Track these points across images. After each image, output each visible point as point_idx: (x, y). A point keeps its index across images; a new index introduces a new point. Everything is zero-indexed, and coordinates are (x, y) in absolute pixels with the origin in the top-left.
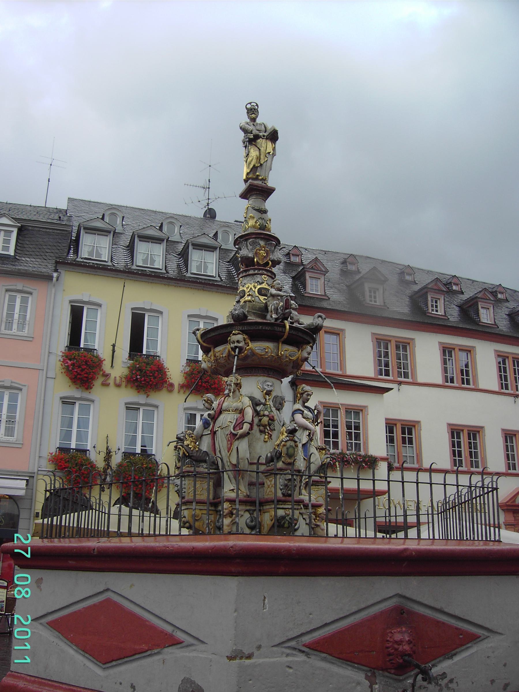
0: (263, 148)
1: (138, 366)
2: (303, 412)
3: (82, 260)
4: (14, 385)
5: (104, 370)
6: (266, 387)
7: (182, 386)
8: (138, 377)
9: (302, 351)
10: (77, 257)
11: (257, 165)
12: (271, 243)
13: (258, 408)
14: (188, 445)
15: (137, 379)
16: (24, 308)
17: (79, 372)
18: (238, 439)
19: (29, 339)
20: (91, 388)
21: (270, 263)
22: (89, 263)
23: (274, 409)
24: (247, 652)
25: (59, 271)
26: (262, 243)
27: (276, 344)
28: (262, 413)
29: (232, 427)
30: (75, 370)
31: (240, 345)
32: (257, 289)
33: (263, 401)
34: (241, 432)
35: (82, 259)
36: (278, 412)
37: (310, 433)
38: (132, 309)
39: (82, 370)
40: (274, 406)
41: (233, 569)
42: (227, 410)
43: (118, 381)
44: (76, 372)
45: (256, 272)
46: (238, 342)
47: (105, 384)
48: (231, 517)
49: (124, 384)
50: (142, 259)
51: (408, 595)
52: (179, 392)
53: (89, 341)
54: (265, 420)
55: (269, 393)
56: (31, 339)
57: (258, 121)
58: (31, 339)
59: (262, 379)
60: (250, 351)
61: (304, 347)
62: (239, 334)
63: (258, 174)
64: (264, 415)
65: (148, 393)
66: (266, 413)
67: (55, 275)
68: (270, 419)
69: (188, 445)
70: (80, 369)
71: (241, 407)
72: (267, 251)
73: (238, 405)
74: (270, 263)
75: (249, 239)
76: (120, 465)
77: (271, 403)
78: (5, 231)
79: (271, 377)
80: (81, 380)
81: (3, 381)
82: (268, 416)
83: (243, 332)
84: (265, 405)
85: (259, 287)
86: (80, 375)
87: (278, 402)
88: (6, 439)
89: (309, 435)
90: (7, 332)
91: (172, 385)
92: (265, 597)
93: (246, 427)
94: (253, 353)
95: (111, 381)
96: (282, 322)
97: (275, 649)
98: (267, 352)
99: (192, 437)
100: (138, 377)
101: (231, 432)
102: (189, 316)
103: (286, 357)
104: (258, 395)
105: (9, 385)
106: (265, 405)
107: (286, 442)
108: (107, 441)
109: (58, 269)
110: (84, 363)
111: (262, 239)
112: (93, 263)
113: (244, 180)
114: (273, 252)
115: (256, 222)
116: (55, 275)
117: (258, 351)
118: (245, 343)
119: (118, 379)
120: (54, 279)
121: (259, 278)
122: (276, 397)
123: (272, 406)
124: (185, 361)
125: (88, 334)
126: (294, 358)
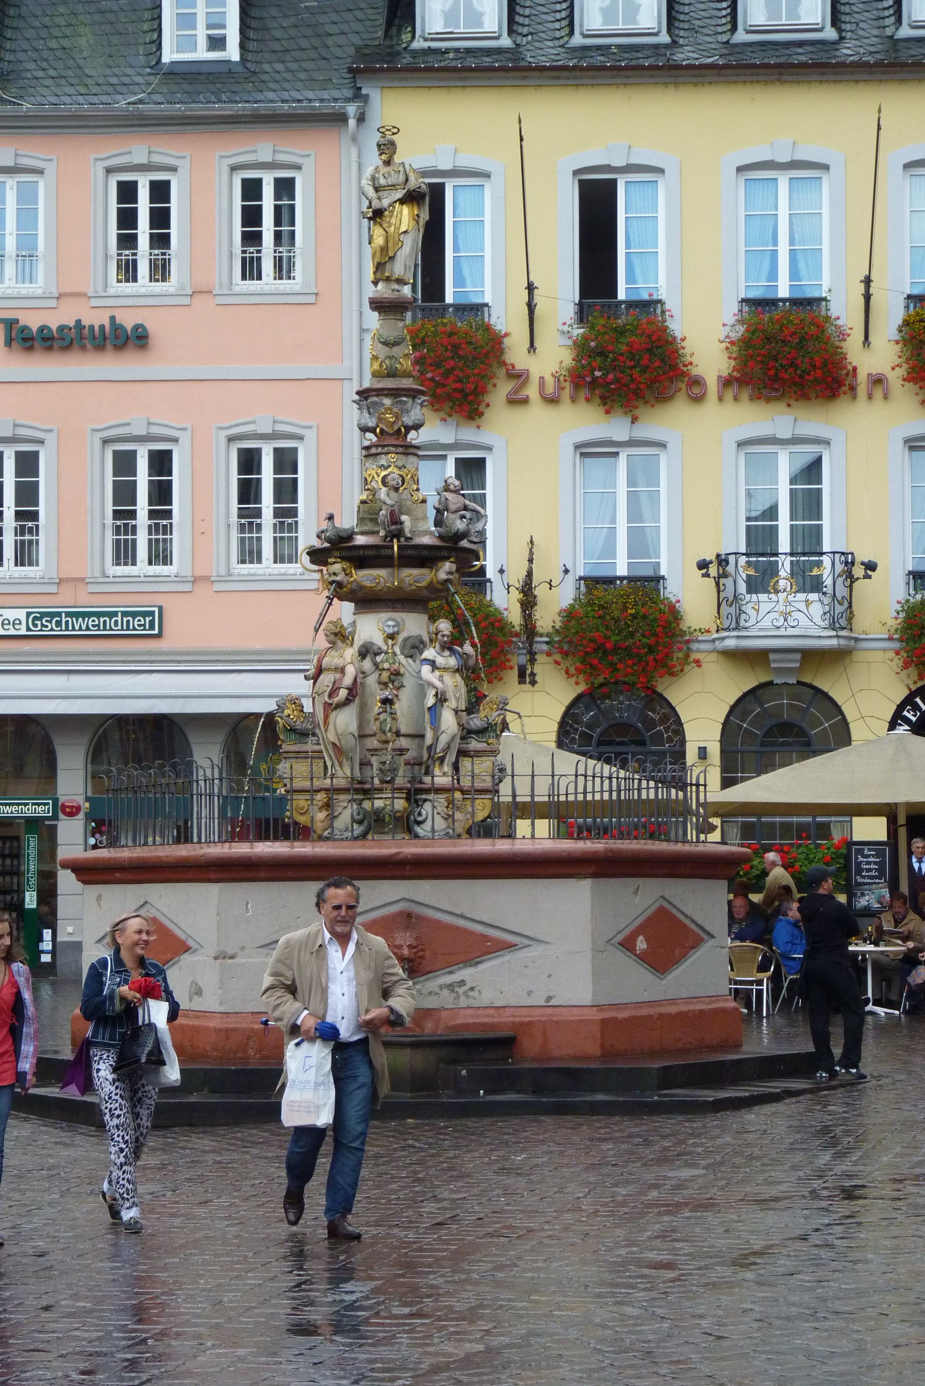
0: (393, 228)
1: (593, 344)
2: (434, 662)
3: (426, 45)
4: (280, 428)
5: (508, 361)
6: (387, 629)
7: (726, 382)
8: (598, 374)
9: (437, 571)
10: (413, 37)
11: (383, 261)
12: (401, 401)
13: (379, 659)
14: (289, 715)
15: (595, 379)
17: (437, 379)
18: (336, 708)
20: (481, 414)
21: (403, 430)
22: (447, 51)
23: (401, 658)
24: (230, 952)
25: (364, 91)
26: (387, 402)
27: (390, 570)
28: (381, 667)
29: (327, 694)
30: (429, 375)
31: (338, 578)
32: (380, 478)
33: (385, 648)
34: (336, 700)
35: (426, 40)
36: (410, 660)
37: (437, 693)
38: (575, 173)
39: (446, 375)
40: (402, 653)
41: (212, 876)
42: (328, 670)
43: (550, 388)
44: (432, 379)
45: (380, 450)
46: (335, 574)
47: (518, 401)
48: (327, 810)
49: (566, 394)
50: (601, 9)
51: (417, 899)
52: (721, 399)
53: (468, 282)
54: (385, 675)
55: (391, 636)
57: (397, 159)
59: (384, 616)
60: (355, 584)
61: (440, 564)
62: (335, 563)
63: (387, 274)
64: (384, 669)
65: (636, 412)
66: (386, 665)
67: (352, 109)
68: (392, 674)
69: (289, 715)
70: (442, 370)
71: (341, 665)
72: (396, 413)
73: (338, 662)
74: (403, 430)
75: (369, 396)
76: (569, 615)
77: (397, 649)
79: (398, 611)
80: (449, 397)
81: (254, 422)
82: (388, 669)
83: (343, 558)
84: (386, 653)
85: (384, 473)
86: (444, 386)
87: (408, 646)
88: (276, 572)
89: (436, 695)
91: (697, 382)
92: (248, 902)
93: (343, 693)
94: (362, 587)
95: (532, 391)
96: (392, 541)
97: (259, 950)
98: (378, 583)
99: (295, 703)
100: (598, 374)
101: (326, 703)
102: (740, 169)
103: (411, 585)
104: (378, 640)
105: (270, 431)
106: (386, 653)
107: (379, 714)
108: (531, 553)
109: (360, 88)
110: (449, 354)
111: (386, 396)
112: (457, 50)
113: (373, 282)
114: (408, 412)
115: (381, 365)
116: (352, 109)
117: (367, 584)
118: (346, 575)
119: (550, 381)
120: (352, 122)
121: (383, 461)
122: (406, 640)
123: (399, 653)
124: (735, 308)
125: (463, 261)
126: (424, 584)
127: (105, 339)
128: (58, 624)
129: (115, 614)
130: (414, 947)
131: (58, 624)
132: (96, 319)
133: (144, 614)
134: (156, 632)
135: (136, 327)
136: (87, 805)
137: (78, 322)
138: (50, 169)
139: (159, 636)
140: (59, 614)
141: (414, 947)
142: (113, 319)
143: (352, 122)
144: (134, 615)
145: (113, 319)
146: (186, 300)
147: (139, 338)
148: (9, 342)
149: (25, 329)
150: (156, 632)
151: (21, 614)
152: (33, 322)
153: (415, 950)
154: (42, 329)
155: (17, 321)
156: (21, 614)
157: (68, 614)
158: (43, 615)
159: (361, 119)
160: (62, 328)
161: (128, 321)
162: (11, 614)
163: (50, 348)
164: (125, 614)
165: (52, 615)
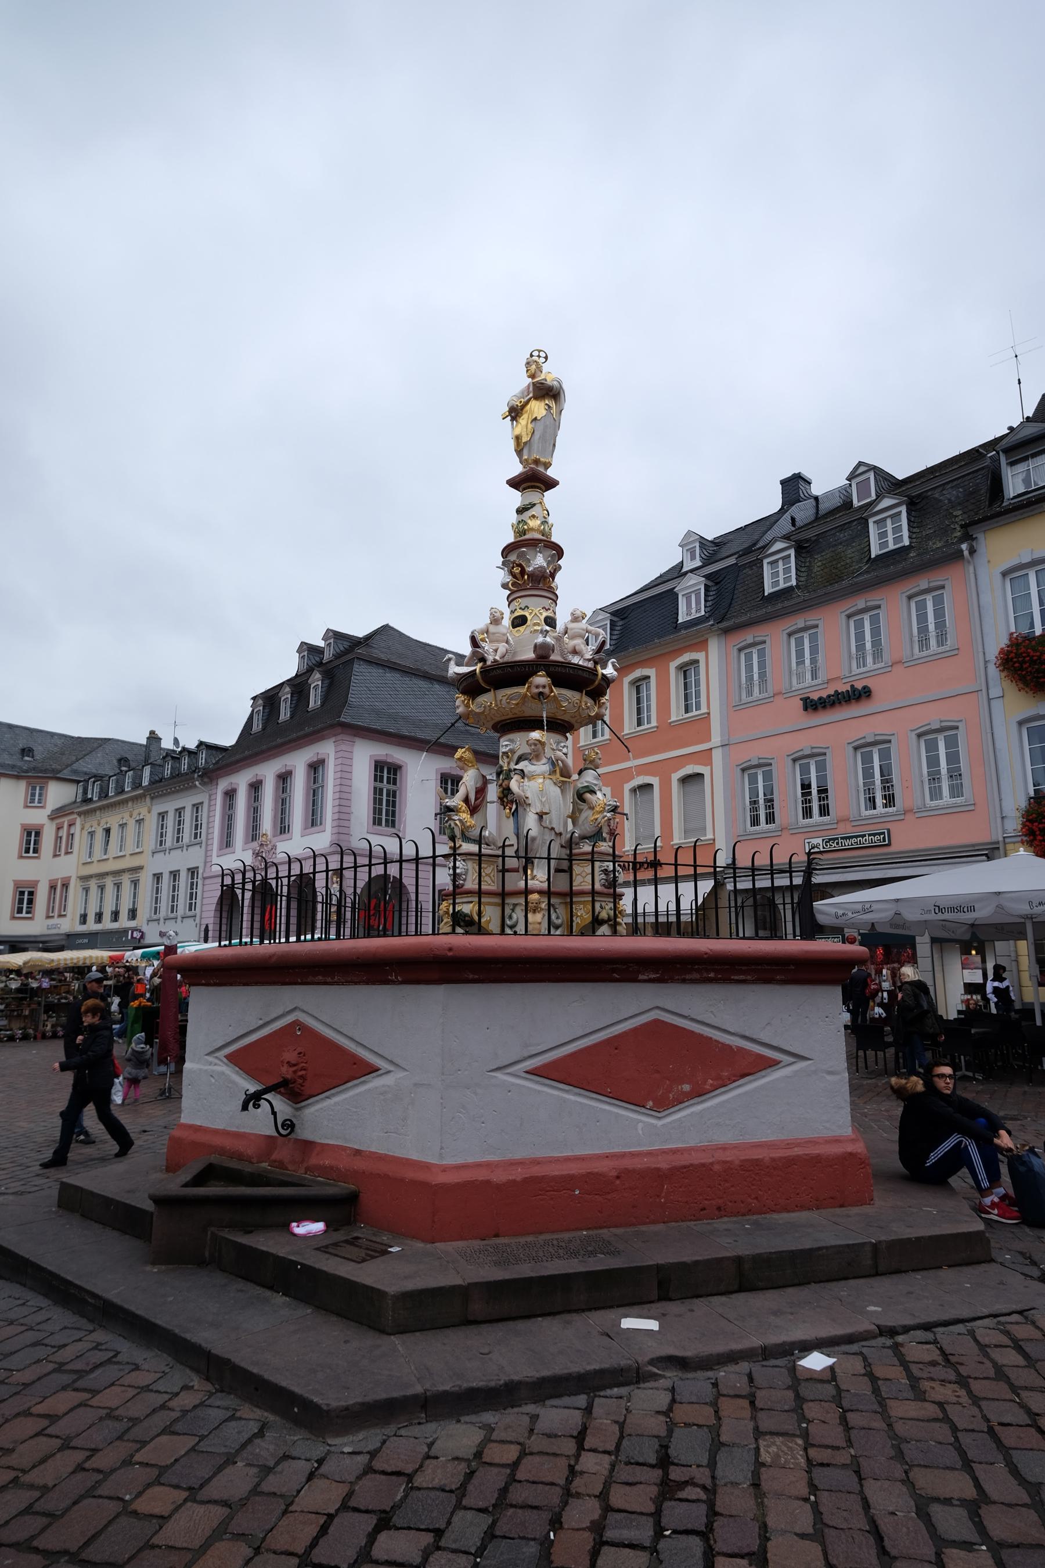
16: (939, 613)
19: (954, 653)
56: (956, 652)
58: (956, 652)
67: (964, 546)
78: (892, 517)
81: (929, 724)
90: (925, 653)
105: (938, 727)
116: (964, 546)
120: (966, 553)
127: (849, 697)
128: (838, 843)
129: (865, 835)
130: (294, 1065)
131: (838, 843)
132: (844, 688)
133: (879, 834)
134: (887, 842)
135: (864, 688)
136: (860, 938)
137: (836, 691)
138: (821, 623)
139: (889, 845)
140: (837, 839)
141: (294, 1065)
142: (852, 686)
143: (966, 553)
144: (874, 835)
145: (852, 686)
146: (889, 669)
147: (865, 693)
148: (806, 709)
149: (812, 700)
150: (887, 842)
151: (819, 841)
152: (815, 696)
153: (294, 1068)
154: (820, 699)
155: (809, 698)
156: (819, 841)
157: (842, 838)
158: (830, 840)
159: (972, 551)
160: (829, 696)
161: (859, 686)
162: (815, 841)
163: (824, 707)
164: (870, 835)
165: (834, 839)
